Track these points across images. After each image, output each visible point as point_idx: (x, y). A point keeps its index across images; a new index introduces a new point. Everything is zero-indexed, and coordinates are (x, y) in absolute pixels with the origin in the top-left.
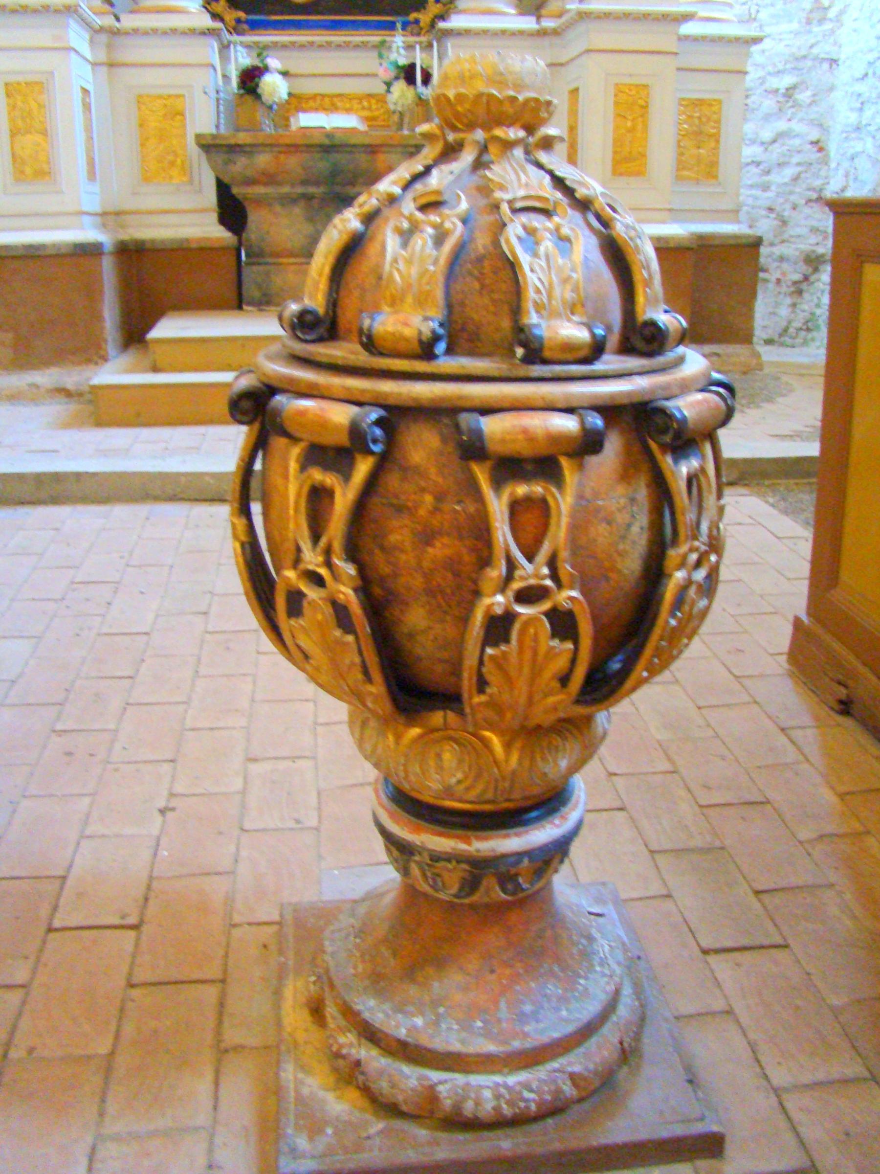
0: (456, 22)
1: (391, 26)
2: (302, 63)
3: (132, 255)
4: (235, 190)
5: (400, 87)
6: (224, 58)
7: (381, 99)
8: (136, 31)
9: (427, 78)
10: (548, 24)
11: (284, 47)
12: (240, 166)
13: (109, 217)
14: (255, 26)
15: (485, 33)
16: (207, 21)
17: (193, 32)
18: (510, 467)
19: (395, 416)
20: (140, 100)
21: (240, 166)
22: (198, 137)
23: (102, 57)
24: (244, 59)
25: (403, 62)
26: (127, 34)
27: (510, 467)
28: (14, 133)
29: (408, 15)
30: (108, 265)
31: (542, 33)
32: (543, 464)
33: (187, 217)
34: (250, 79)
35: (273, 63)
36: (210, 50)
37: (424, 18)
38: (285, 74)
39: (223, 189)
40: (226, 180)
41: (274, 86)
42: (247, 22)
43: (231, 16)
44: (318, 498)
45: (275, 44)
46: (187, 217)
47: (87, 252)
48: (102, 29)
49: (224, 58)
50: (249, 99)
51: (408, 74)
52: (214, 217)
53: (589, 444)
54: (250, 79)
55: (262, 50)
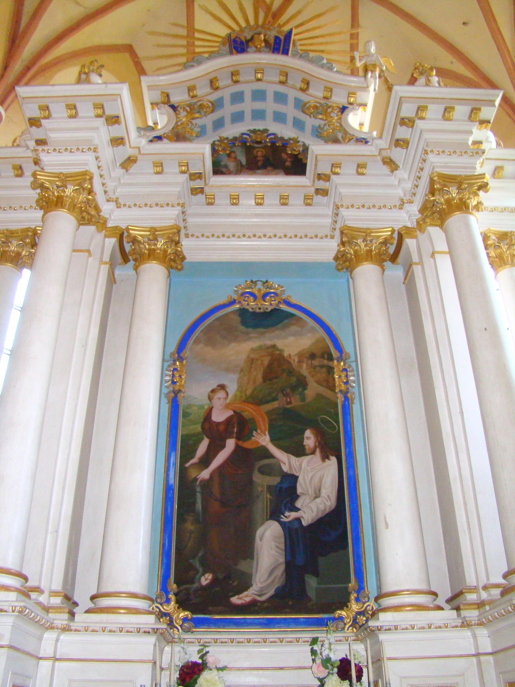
14: (198, 623)
29: (333, 612)
42: (192, 620)
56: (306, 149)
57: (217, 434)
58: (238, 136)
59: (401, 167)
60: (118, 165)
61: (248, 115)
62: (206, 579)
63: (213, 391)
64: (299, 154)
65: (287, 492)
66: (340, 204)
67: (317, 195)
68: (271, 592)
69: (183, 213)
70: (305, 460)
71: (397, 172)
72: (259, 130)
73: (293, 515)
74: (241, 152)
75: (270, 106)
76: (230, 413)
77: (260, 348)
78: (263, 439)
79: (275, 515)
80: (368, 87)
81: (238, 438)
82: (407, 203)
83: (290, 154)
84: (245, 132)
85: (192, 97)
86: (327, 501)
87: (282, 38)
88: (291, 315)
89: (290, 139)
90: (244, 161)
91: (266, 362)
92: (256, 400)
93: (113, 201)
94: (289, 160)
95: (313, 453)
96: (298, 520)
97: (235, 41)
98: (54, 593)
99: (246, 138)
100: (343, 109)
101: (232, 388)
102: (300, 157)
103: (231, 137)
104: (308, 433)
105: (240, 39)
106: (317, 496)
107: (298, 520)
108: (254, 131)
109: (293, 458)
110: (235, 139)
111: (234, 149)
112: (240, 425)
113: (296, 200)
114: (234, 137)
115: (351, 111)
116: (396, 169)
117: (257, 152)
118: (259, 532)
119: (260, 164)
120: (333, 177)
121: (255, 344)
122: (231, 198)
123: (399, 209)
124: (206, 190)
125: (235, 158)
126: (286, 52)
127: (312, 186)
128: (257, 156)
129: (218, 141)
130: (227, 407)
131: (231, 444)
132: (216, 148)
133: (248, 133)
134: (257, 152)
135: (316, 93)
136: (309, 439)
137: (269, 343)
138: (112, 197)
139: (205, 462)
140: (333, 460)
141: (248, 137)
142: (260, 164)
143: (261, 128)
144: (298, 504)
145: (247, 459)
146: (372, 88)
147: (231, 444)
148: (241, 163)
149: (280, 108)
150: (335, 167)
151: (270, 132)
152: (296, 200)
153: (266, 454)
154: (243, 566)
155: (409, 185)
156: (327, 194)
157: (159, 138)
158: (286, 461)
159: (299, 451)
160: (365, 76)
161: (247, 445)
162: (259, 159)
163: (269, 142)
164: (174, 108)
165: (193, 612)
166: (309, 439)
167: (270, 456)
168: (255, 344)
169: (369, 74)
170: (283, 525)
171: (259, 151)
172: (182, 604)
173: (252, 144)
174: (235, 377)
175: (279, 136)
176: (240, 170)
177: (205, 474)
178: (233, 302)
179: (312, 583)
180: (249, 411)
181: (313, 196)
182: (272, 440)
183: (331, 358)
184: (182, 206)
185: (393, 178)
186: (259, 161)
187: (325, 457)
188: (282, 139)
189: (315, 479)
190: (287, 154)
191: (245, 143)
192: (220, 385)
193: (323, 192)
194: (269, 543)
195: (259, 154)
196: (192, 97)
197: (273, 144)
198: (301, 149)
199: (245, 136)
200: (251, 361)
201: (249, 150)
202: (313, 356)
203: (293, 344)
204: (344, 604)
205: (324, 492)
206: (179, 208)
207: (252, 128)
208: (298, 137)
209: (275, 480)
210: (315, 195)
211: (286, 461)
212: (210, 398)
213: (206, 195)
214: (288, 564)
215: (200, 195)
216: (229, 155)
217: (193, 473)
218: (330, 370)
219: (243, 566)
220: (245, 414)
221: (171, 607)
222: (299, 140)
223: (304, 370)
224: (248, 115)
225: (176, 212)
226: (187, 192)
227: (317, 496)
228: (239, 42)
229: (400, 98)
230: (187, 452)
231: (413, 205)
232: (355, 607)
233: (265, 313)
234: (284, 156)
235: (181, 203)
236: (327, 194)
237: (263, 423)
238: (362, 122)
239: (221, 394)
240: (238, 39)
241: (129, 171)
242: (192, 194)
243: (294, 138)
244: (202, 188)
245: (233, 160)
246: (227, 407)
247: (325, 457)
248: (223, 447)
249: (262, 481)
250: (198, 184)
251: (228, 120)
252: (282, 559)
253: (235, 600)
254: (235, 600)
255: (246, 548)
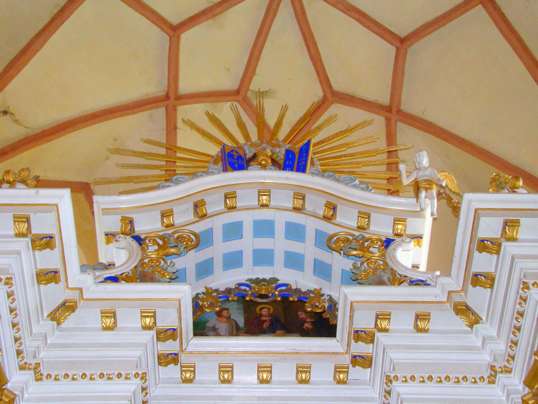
56: (333, 305)
58: (233, 287)
59: (484, 318)
60: (45, 315)
61: (248, 258)
64: (324, 312)
66: (392, 375)
67: (354, 366)
69: (143, 389)
71: (478, 325)
72: (264, 280)
74: (238, 309)
75: (280, 244)
80: (422, 210)
82: (502, 372)
83: (310, 312)
84: (244, 282)
85: (167, 226)
87: (297, 151)
89: (310, 291)
90: (241, 322)
93: (29, 369)
94: (308, 320)
97: (230, 155)
99: (245, 290)
100: (388, 242)
102: (326, 315)
103: (222, 289)
105: (237, 152)
108: (257, 281)
110: (229, 291)
111: (227, 305)
113: (322, 373)
114: (226, 289)
115: (399, 245)
116: (477, 322)
117: (261, 309)
119: (265, 325)
120: (378, 335)
122: (220, 371)
123: (489, 382)
124: (183, 358)
125: (229, 318)
126: (302, 169)
127: (347, 353)
128: (261, 315)
129: (203, 293)
132: (201, 303)
133: (248, 282)
134: (261, 309)
135: (348, 219)
138: (29, 362)
141: (248, 289)
142: (265, 325)
143: (267, 277)
146: (428, 212)
148: (237, 325)
149: (295, 247)
150: (381, 319)
151: (279, 282)
152: (322, 373)
155: (501, 346)
156: (370, 366)
157: (114, 279)
160: (417, 196)
162: (264, 318)
163: (279, 295)
164: (138, 239)
169: (423, 194)
171: (264, 308)
173: (253, 299)
175: (294, 287)
176: (236, 331)
181: (348, 368)
184: (142, 378)
185: (473, 336)
186: (265, 321)
188: (298, 291)
190: (306, 312)
191: (244, 297)
193: (363, 361)
195: (265, 312)
196: (167, 226)
197: (285, 298)
198: (326, 305)
199: (243, 288)
201: (249, 307)
206: (138, 381)
207: (254, 277)
208: (321, 289)
210: (351, 365)
213: (182, 367)
215: (173, 365)
216: (219, 314)
222: (322, 292)
224: (248, 258)
225: (133, 388)
226: (152, 360)
228: (235, 157)
229: (476, 210)
231: (512, 375)
234: (301, 315)
235: (140, 373)
236: (370, 366)
238: (416, 263)
240: (234, 153)
241: (63, 326)
242: (160, 364)
243: (315, 290)
244: (176, 354)
245: (224, 319)
250: (170, 346)
251: (218, 263)
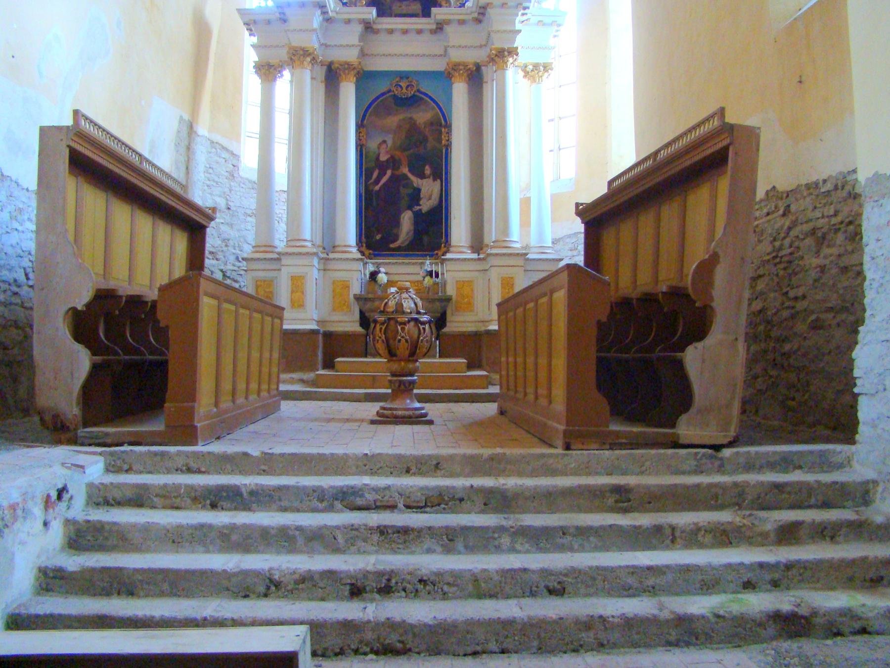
0: (449, 256)
1: (426, 255)
2: (394, 269)
3: (329, 336)
4: (367, 314)
5: (428, 279)
6: (365, 268)
7: (421, 282)
8: (334, 259)
9: (437, 276)
10: (482, 256)
11: (387, 264)
12: (369, 305)
13: (318, 322)
15: (458, 259)
16: (359, 256)
17: (354, 259)
18: (401, 324)
19: (389, 319)
20: (334, 283)
21: (369, 305)
22: (355, 295)
23: (322, 267)
24: (371, 268)
25: (429, 269)
26: (331, 260)
27: (401, 324)
28: (292, 292)
30: (320, 338)
31: (479, 259)
32: (404, 324)
33: (348, 323)
34: (374, 275)
35: (382, 270)
36: (360, 266)
37: (440, 253)
38: (386, 273)
39: (361, 312)
40: (364, 310)
41: (382, 278)
43: (367, 252)
44: (381, 329)
45: (383, 263)
46: (348, 323)
47: (313, 332)
48: (323, 259)
49: (365, 268)
50: (373, 282)
51: (430, 274)
52: (358, 324)
53: (409, 322)
54: (374, 275)
55: (378, 265)
57: (382, 167)
62: (378, 237)
63: (380, 144)
65: (416, 196)
68: (407, 243)
70: (425, 181)
73: (418, 208)
76: (389, 156)
77: (404, 120)
78: (405, 170)
79: (410, 208)
81: (393, 169)
86: (434, 201)
88: (421, 99)
91: (408, 126)
92: (403, 149)
95: (429, 177)
96: (420, 210)
98: (319, 246)
101: (390, 142)
104: (427, 167)
106: (430, 199)
107: (420, 210)
109: (419, 180)
112: (393, 162)
118: (402, 216)
121: (401, 117)
130: (387, 152)
131: (389, 173)
136: (428, 170)
137: (409, 115)
139: (377, 181)
140: (439, 181)
144: (421, 202)
145: (398, 180)
147: (389, 173)
153: (405, 177)
154: (395, 231)
158: (416, 181)
159: (422, 176)
161: (397, 173)
165: (374, 250)
166: (428, 170)
167: (408, 178)
168: (401, 117)
170: (414, 212)
172: (368, 247)
174: (391, 136)
177: (377, 188)
178: (389, 91)
179: (426, 239)
180: (398, 154)
182: (410, 171)
183: (441, 125)
187: (435, 180)
189: (429, 189)
192: (384, 144)
194: (407, 220)
200: (399, 127)
202: (432, 124)
203: (422, 117)
204: (439, 248)
205: (433, 197)
209: (410, 191)
211: (416, 181)
212: (379, 148)
214: (415, 230)
217: (371, 188)
218: (440, 133)
219: (395, 231)
220: (396, 157)
221: (364, 249)
223: (427, 132)
227: (430, 199)
230: (368, 176)
232: (443, 249)
233: (406, 98)
237: (405, 162)
239: (384, 146)
246: (387, 152)
247: (435, 180)
248: (385, 174)
249: (404, 191)
252: (412, 228)
253: (392, 246)
254: (392, 246)
255: (396, 223)
